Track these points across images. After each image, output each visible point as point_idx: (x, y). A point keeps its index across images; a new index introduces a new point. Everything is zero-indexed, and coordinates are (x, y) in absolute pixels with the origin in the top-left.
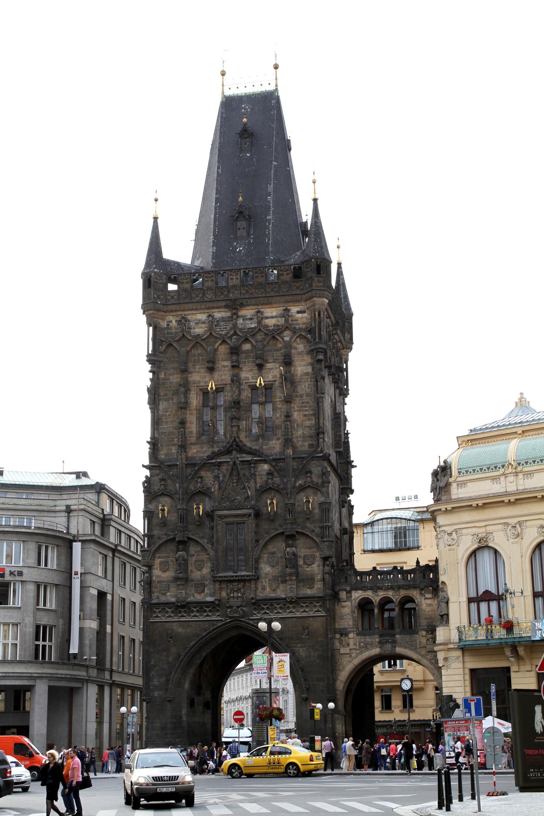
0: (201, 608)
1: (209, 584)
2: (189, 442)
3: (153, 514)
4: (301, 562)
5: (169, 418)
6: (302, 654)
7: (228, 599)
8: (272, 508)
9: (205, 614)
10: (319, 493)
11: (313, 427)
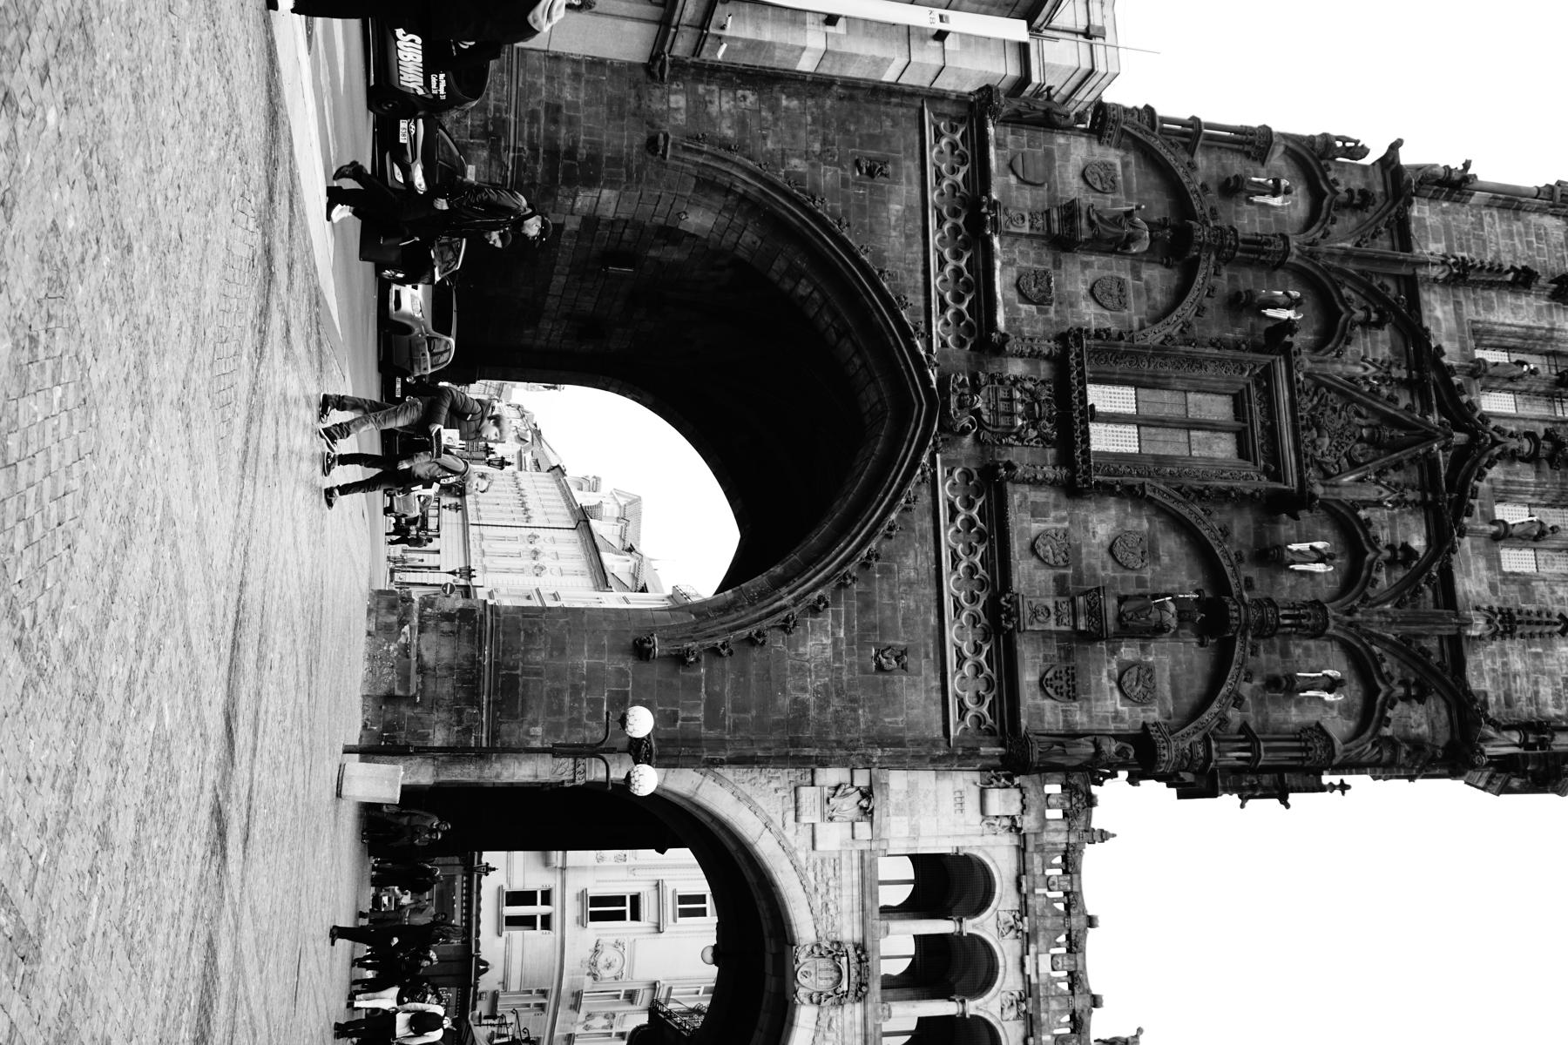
0: (968, 286)
1: (1048, 321)
2: (1462, 298)
3: (1255, 159)
4: (1128, 652)
5: (1521, 241)
6: (810, 643)
7: (1001, 382)
8: (1303, 557)
9: (948, 296)
10: (1352, 724)
11: (1537, 709)
